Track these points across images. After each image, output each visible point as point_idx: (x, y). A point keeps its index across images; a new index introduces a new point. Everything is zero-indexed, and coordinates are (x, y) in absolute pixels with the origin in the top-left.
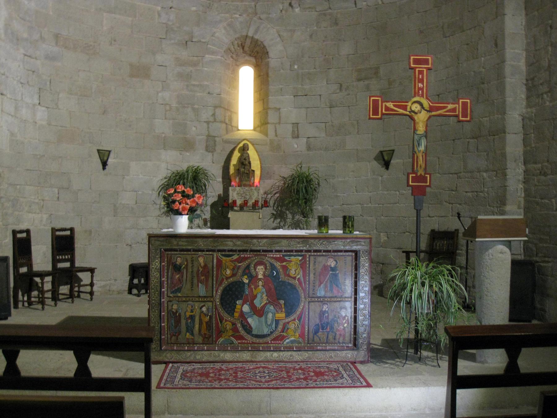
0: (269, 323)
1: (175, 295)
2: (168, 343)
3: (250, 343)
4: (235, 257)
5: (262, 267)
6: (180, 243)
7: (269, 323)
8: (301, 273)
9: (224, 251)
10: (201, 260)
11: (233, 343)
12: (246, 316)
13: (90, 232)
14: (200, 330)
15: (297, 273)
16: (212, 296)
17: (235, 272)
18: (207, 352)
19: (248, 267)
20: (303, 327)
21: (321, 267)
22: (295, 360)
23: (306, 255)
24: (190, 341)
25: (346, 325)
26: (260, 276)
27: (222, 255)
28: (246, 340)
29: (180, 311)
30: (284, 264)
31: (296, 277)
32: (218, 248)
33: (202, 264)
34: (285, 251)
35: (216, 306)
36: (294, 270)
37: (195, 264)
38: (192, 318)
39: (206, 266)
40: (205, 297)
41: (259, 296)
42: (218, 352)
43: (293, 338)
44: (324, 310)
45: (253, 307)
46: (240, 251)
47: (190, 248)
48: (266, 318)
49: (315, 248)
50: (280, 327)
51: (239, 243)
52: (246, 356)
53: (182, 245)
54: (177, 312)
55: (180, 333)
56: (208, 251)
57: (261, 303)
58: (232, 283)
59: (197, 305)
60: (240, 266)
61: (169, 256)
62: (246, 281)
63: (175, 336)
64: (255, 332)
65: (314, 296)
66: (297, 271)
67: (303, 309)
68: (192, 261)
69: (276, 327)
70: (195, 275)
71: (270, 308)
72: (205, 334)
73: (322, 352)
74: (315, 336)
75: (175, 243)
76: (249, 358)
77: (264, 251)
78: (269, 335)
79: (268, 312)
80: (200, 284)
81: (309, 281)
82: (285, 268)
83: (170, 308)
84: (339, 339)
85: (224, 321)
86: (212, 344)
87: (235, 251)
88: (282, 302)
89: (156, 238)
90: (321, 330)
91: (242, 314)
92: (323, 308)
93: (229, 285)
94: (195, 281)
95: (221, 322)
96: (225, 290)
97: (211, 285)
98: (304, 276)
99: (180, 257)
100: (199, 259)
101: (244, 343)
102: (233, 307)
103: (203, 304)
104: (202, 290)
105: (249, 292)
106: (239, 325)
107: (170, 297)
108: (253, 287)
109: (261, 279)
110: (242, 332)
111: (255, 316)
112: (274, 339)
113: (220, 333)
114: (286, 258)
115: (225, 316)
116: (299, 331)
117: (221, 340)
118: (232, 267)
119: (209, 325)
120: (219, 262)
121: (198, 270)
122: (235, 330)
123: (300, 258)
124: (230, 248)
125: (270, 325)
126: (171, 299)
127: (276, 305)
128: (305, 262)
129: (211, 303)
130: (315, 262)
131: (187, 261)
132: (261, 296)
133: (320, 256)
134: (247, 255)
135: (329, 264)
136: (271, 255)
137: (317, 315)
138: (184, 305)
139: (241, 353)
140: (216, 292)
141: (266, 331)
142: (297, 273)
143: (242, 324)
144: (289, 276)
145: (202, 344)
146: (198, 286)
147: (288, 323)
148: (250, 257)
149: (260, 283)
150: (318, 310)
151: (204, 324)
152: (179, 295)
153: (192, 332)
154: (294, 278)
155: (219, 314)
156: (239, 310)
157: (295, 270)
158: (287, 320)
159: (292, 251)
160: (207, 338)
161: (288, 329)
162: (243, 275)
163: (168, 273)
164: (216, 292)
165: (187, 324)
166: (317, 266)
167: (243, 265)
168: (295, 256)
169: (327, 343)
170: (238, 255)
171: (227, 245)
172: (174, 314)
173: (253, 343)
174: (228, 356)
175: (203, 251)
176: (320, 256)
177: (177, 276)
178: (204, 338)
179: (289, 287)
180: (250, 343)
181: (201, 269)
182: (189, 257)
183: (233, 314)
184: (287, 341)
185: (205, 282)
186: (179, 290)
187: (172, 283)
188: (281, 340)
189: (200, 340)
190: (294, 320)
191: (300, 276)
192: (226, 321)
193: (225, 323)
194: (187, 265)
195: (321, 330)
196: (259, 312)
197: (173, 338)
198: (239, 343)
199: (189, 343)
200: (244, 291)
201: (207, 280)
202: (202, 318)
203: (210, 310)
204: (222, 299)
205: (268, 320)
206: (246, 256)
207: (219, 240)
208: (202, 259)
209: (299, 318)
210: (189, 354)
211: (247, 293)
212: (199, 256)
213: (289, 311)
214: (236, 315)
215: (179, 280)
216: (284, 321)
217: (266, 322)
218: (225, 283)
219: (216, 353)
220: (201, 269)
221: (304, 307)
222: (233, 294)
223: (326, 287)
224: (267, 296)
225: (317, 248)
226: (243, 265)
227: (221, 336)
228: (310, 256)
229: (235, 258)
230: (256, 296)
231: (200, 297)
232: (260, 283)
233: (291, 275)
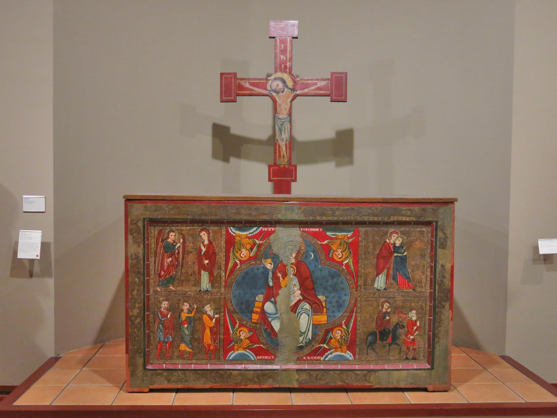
12: (270, 319)
30: (326, 242)
31: (343, 261)
44: (384, 310)
80: (202, 271)
91: (263, 314)
100: (202, 234)
105: (274, 283)
108: (279, 275)
118: (249, 247)
154: (341, 263)
156: (259, 310)
161: (331, 338)
181: (204, 249)
214: (255, 317)
220: (204, 249)
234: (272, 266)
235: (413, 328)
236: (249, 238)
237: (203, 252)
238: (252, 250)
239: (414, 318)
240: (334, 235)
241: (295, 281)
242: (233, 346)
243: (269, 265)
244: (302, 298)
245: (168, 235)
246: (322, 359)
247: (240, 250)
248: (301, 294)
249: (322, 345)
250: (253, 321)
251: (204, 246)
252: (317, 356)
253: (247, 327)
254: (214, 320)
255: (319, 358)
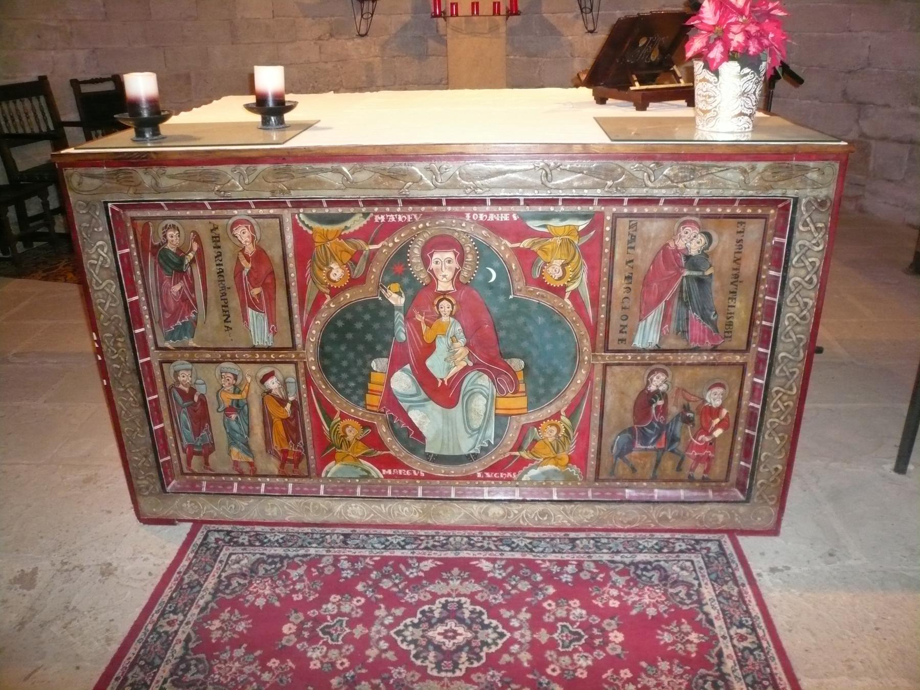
0: (476, 423)
1: (179, 343)
2: (183, 473)
3: (419, 477)
4: (356, 223)
5: (450, 255)
6: (165, 182)
7: (476, 424)
8: (584, 276)
9: (317, 203)
10: (244, 235)
11: (368, 476)
12: (405, 405)
13: (188, 77)
14: (268, 442)
15: (570, 274)
16: (294, 347)
17: (358, 271)
18: (293, 501)
19: (402, 254)
20: (584, 434)
21: (650, 257)
22: (554, 523)
23: (601, 215)
24: (246, 469)
25: (718, 433)
26: (444, 285)
27: (310, 217)
28: (407, 468)
29: (201, 389)
30: (525, 244)
31: (565, 287)
32: (294, 194)
33: (250, 250)
34: (529, 202)
35: (307, 374)
36: (557, 263)
37: (227, 248)
38: (238, 407)
39: (260, 256)
40: (269, 349)
41: (442, 345)
42: (327, 501)
43: (549, 467)
44: (653, 388)
45: (424, 378)
46: (369, 203)
47: (197, 196)
48: (467, 410)
49: (635, 192)
50: (511, 436)
51: (363, 176)
52: (407, 512)
53: (172, 190)
54: (193, 391)
55: (209, 449)
56: (260, 204)
57: (449, 369)
58: (351, 308)
59: (251, 373)
60: (373, 253)
61: (140, 223)
62: (397, 300)
63: (198, 454)
64: (432, 448)
65: (623, 347)
66: (569, 268)
67: (586, 385)
68: (216, 239)
69: (497, 436)
70: (230, 281)
71: (480, 381)
72: (285, 452)
73: (640, 506)
74: (619, 460)
75: (147, 180)
76: (417, 518)
77: (451, 202)
78: (476, 456)
79: (473, 394)
80: (250, 311)
81: (609, 303)
82: (526, 258)
83: (170, 380)
84: (692, 470)
85: (337, 418)
86: (309, 476)
87: (353, 203)
88: (517, 364)
89: (81, 170)
90: (638, 445)
92: (648, 383)
93: (340, 316)
94: (234, 302)
95: (329, 419)
96: (330, 327)
97: (285, 314)
98: (594, 287)
99: (174, 227)
101: (403, 477)
102: (360, 379)
103: (267, 370)
104: (258, 329)
105: (408, 334)
106: (383, 430)
107: (166, 349)
108: (419, 318)
109: (444, 293)
110: (396, 449)
111: (432, 406)
112: (493, 468)
113: (327, 450)
114: (534, 224)
115: (339, 402)
116: (571, 447)
117: (332, 468)
118: (346, 257)
119: (292, 427)
120: (304, 241)
121: (239, 269)
122: (373, 440)
123: (582, 224)
124: (333, 194)
125: (479, 430)
126: (170, 355)
127: (498, 374)
128: (600, 236)
129: (291, 367)
130: (633, 238)
131: (198, 239)
132: (449, 348)
133: (650, 216)
134: (397, 215)
135: (681, 244)
136: (480, 213)
137: (630, 404)
138: (210, 373)
139: (392, 505)
140: (305, 332)
141: (466, 446)
142: (570, 274)
143: (391, 425)
144: (541, 283)
145: (278, 476)
146: (245, 318)
147: (537, 424)
148: (405, 223)
149: (445, 307)
150: (634, 388)
151: (279, 427)
152: (192, 343)
153: (247, 444)
154: (559, 291)
155: (318, 395)
156: (382, 389)
157: (563, 266)
158: (533, 417)
159: (553, 201)
160: (291, 461)
161: (535, 441)
162: (383, 285)
163: (144, 277)
164: (305, 332)
165: (226, 425)
166: (639, 251)
167: (386, 247)
168: (563, 217)
169: (654, 479)
170: (365, 215)
171: (320, 184)
172: (188, 395)
173: (429, 477)
174: (356, 511)
175: (246, 206)
176: (650, 216)
177: (176, 288)
178: (284, 461)
179: (540, 320)
180: (419, 477)
181: (247, 266)
182: (202, 228)
183: (363, 398)
184: (533, 472)
185: (267, 305)
186: (190, 329)
187: (165, 309)
188: (515, 469)
189: (273, 466)
190: (557, 416)
191: (581, 284)
192: (343, 416)
193: (342, 424)
194: (200, 253)
195: (638, 445)
196: (445, 394)
197: (196, 460)
198: (387, 476)
199: (241, 474)
200: (392, 332)
201: (271, 299)
202: (272, 407)
203: (292, 388)
204: (323, 355)
205: (472, 415)
206: (392, 218)
207: (294, 166)
208: (248, 233)
209: (571, 412)
210: (243, 503)
211: (403, 337)
212: (236, 224)
213: (541, 391)
214: (374, 400)
215: (184, 299)
216: (524, 420)
217: (467, 421)
218: (330, 307)
219: (322, 503)
220: (247, 266)
221: (589, 379)
222: (354, 340)
223: (666, 318)
224: (467, 345)
225: (642, 192)
226: (386, 247)
227: (331, 458)
228: (616, 217)
229: (357, 228)
230: (430, 348)
231: (254, 348)
232: (445, 307)
233: (549, 281)
234: (403, 300)
235: (711, 423)
236: (346, 238)
237: (245, 273)
238: (356, 264)
239: (717, 403)
240: (545, 226)
241: (457, 328)
242: (334, 453)
243: (395, 296)
244: (471, 364)
245: (165, 236)
246: (515, 476)
247: (327, 265)
248: (470, 356)
249: (517, 453)
250: (368, 407)
251: (246, 257)
252: (505, 472)
253: (356, 419)
254: (289, 405)
255: (509, 475)
